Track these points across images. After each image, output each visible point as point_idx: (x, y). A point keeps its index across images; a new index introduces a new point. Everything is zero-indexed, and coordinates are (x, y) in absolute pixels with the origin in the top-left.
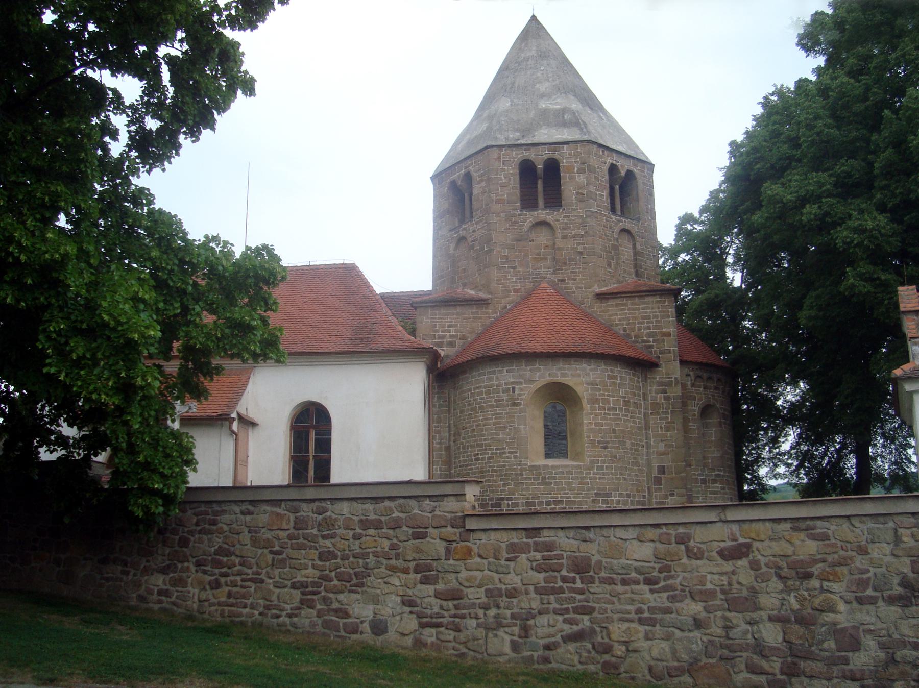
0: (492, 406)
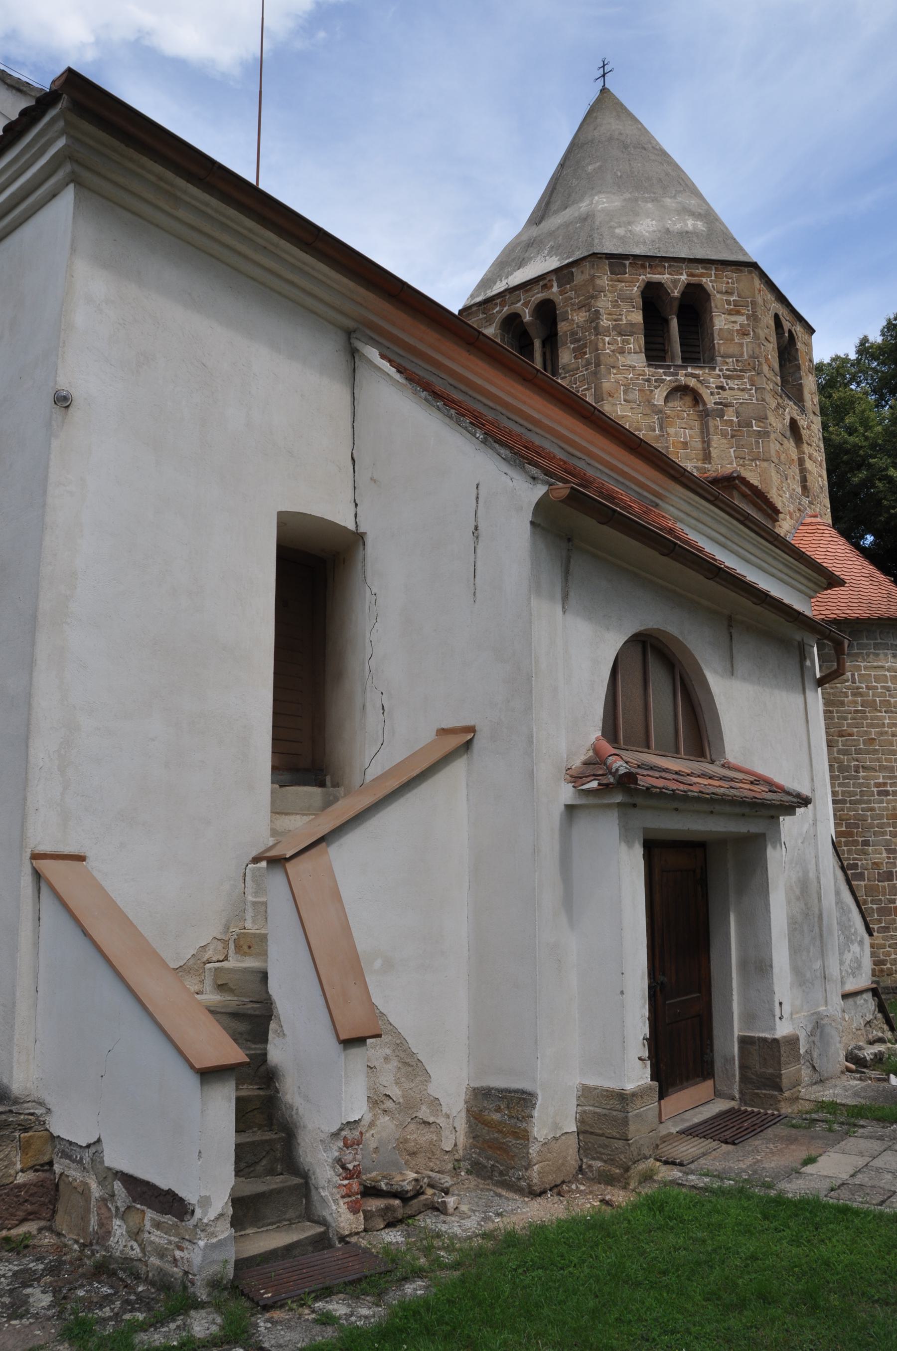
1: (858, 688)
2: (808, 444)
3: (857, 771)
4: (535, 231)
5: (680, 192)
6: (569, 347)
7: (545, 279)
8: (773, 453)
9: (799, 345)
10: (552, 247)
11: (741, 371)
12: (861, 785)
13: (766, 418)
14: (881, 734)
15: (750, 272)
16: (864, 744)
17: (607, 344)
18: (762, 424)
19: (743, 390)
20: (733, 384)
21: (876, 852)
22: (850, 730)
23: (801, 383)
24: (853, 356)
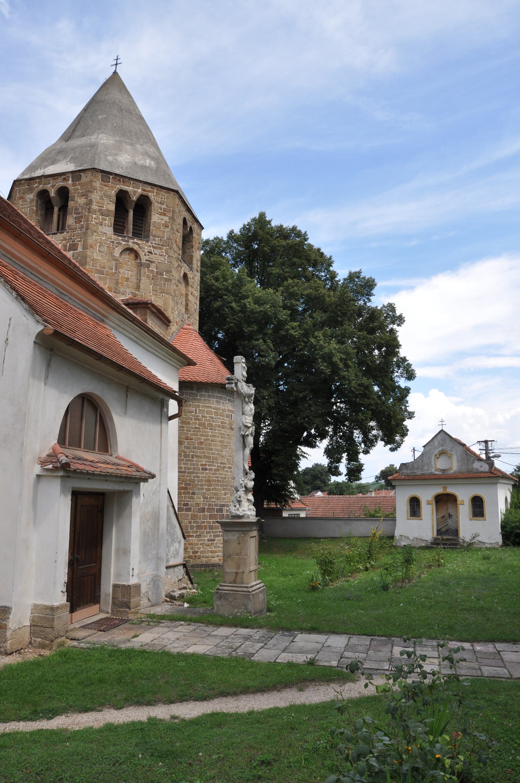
0: (219, 426)
1: (198, 416)
2: (191, 287)
3: (193, 458)
4: (64, 145)
5: (146, 143)
6: (73, 216)
7: (65, 175)
8: (172, 291)
9: (195, 235)
10: (72, 157)
11: (162, 245)
12: (194, 464)
13: (171, 272)
14: (207, 440)
15: (174, 195)
16: (198, 444)
17: (94, 219)
18: (168, 275)
19: (161, 255)
20: (157, 251)
21: (198, 498)
22: (191, 437)
23: (192, 255)
24: (225, 239)
